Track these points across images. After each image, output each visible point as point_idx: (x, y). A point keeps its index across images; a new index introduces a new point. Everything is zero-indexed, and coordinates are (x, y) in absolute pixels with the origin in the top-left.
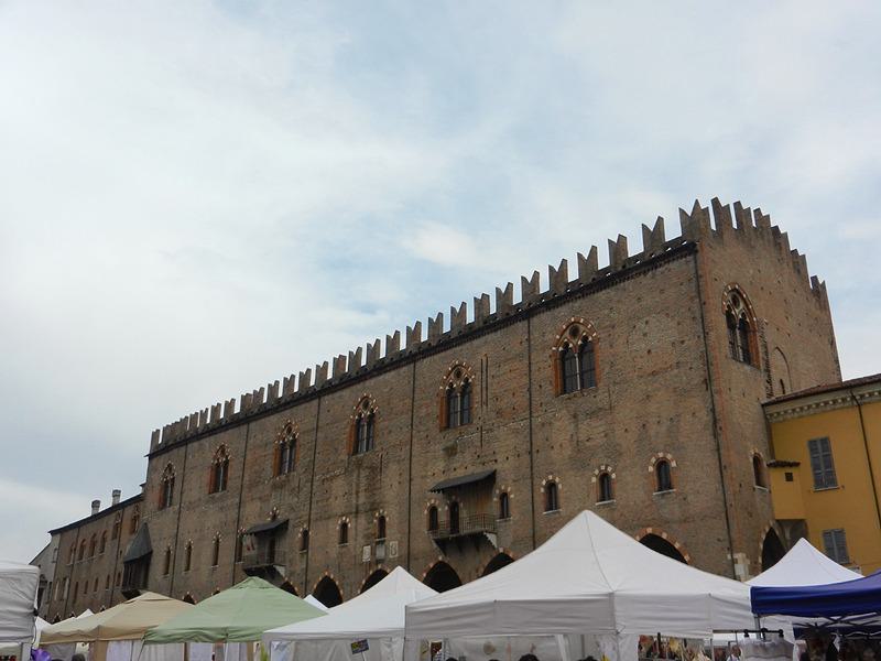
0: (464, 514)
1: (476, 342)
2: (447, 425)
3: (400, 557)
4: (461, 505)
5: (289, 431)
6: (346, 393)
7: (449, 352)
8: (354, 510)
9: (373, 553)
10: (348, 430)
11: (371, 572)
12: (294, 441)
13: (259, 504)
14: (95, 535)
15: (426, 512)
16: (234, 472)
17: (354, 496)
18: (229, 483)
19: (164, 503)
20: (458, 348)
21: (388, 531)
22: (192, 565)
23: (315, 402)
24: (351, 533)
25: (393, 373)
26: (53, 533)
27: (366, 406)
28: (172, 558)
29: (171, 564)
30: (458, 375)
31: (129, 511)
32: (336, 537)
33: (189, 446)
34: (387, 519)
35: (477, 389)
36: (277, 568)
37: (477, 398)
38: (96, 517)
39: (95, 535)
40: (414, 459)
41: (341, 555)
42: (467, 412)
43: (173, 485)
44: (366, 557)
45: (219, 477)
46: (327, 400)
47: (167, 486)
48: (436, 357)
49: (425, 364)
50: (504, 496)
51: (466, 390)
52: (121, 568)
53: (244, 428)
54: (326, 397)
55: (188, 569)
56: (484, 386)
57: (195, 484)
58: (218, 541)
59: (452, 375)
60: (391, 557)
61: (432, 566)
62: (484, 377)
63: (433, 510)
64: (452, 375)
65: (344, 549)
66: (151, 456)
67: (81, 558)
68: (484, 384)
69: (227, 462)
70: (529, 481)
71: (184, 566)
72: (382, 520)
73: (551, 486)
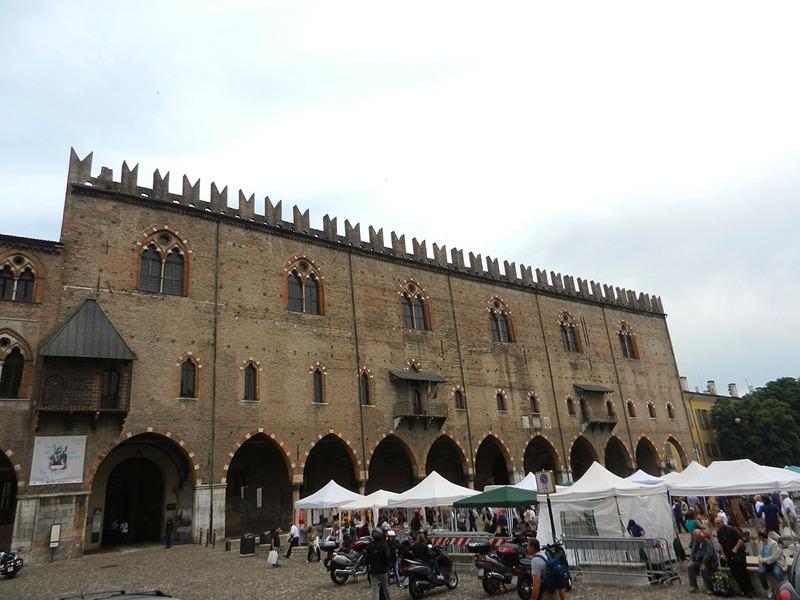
0: (590, 409)
1: (574, 304)
4: (587, 402)
7: (557, 300)
9: (531, 423)
11: (532, 437)
13: (387, 347)
17: (506, 374)
20: (564, 302)
21: (540, 408)
32: (495, 404)
35: (582, 334)
41: (500, 418)
44: (526, 424)
50: (609, 404)
58: (318, 374)
65: (504, 416)
66: (75, 190)
72: (533, 398)
73: (630, 405)
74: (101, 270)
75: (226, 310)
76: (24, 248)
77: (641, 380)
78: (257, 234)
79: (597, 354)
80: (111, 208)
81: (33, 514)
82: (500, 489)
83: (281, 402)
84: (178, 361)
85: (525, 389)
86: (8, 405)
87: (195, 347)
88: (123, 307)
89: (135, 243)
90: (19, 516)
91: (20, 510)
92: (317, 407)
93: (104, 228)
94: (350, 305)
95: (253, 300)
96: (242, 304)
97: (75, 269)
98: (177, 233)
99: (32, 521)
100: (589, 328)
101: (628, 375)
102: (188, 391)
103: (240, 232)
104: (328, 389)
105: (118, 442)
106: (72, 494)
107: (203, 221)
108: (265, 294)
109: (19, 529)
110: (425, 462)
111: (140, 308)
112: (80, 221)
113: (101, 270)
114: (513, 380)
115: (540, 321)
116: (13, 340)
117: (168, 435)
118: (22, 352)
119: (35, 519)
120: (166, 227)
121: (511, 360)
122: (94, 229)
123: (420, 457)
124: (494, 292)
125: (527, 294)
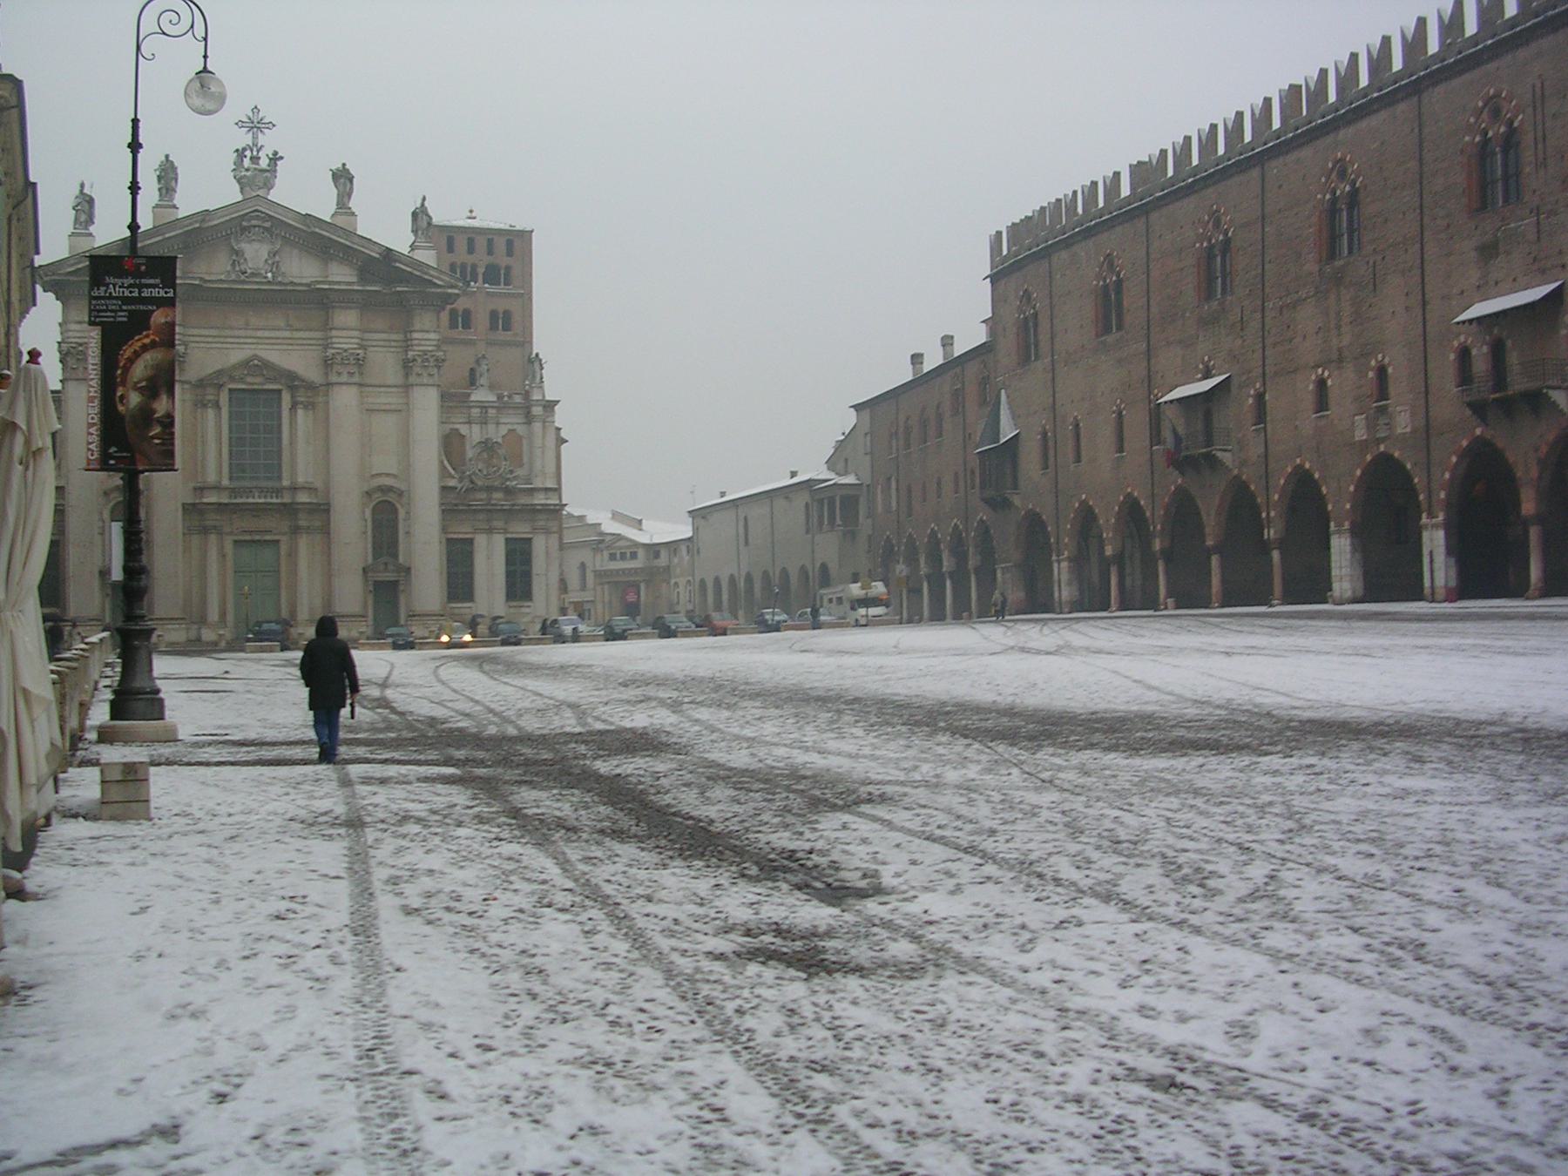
0: (1513, 359)
2: (1481, 202)
3: (1414, 431)
4: (1509, 343)
5: (1217, 224)
6: (1306, 153)
8: (1335, 357)
10: (1314, 219)
11: (1369, 458)
12: (1227, 241)
14: (924, 409)
15: (1452, 356)
16: (1132, 299)
18: (1128, 319)
19: (1027, 352)
20: (1491, 67)
21: (1392, 391)
22: (1083, 453)
23: (1255, 173)
24: (1334, 395)
25: (1383, 115)
26: (858, 407)
27: (1342, 174)
28: (1051, 444)
29: (1051, 453)
30: (1496, 113)
31: (973, 369)
32: (1309, 401)
33: (1055, 258)
34: (1390, 370)
35: (1528, 139)
36: (1219, 454)
37: (1528, 156)
38: (921, 381)
39: (924, 409)
40: (1428, 268)
42: (1512, 179)
43: (1036, 325)
44: (1360, 434)
45: (1109, 309)
46: (1275, 167)
47: (1028, 330)
48: (1456, 82)
49: (1436, 97)
51: (1510, 142)
52: (975, 463)
53: (1140, 224)
54: (1274, 163)
55: (1078, 460)
56: (1540, 134)
57: (1074, 322)
58: (1120, 414)
59: (1485, 115)
60: (1399, 431)
61: (1465, 443)
62: (1539, 117)
63: (1464, 354)
64: (1485, 115)
65: (1323, 422)
66: (995, 278)
67: (908, 446)
68: (1540, 127)
69: (1119, 282)
71: (1071, 457)
72: (1382, 371)
82: (1167, 573)
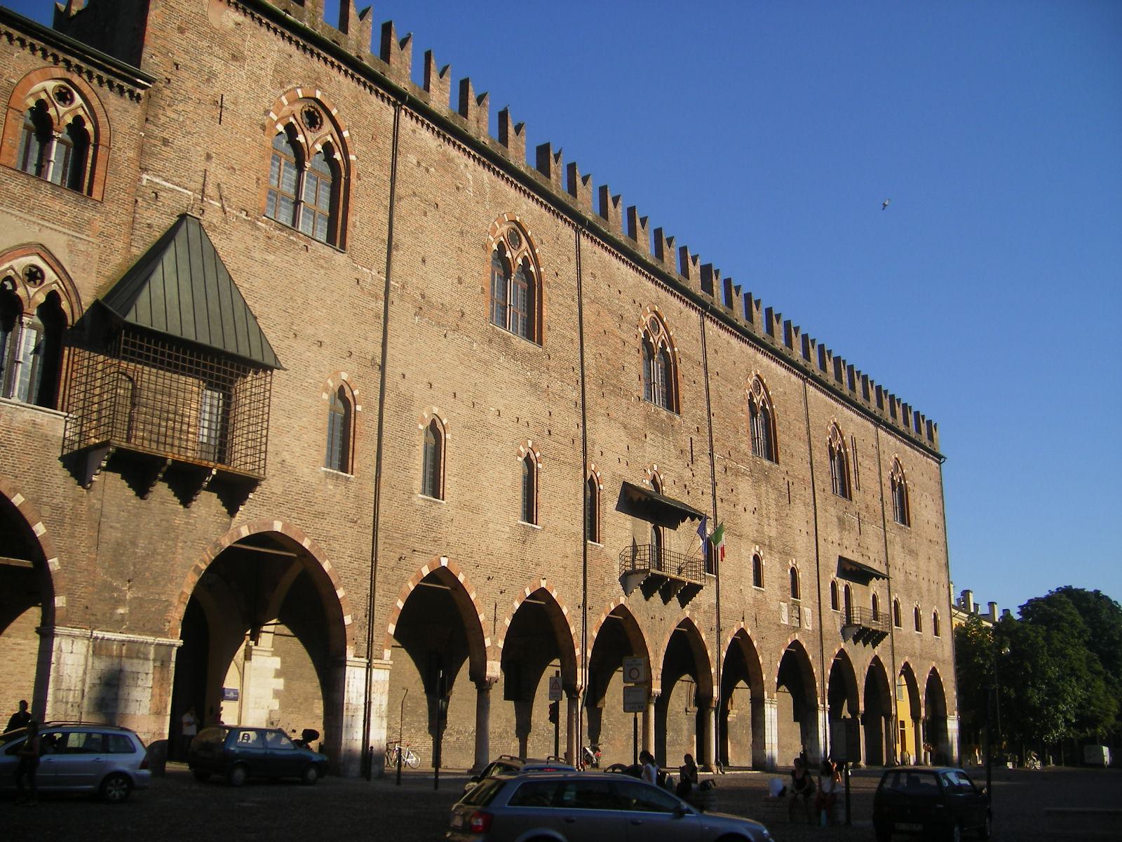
13: (622, 433)
17: (765, 520)
44: (785, 620)
63: (834, 585)
65: (760, 596)
70: (887, 591)
74: (209, 157)
75: (402, 297)
76: (79, 70)
77: (910, 566)
78: (453, 152)
79: (867, 507)
80: (231, 25)
81: (81, 672)
83: (475, 510)
84: (326, 389)
85: (786, 553)
86: (38, 421)
87: (352, 365)
88: (241, 247)
89: (267, 112)
90: (58, 672)
91: (59, 659)
92: (527, 532)
93: (218, 66)
94: (576, 336)
95: (440, 286)
96: (427, 293)
97: (165, 142)
98: (334, 112)
99: (79, 686)
100: (860, 459)
101: (897, 553)
102: (342, 457)
103: (427, 138)
104: (542, 497)
105: (226, 542)
106: (150, 639)
107: (373, 97)
108: (460, 281)
109: (56, 701)
110: (661, 667)
111: (271, 257)
112: (176, 37)
113: (209, 157)
114: (773, 534)
115: (809, 433)
116: (50, 275)
117: (306, 544)
118: (65, 305)
119: (84, 681)
120: (318, 95)
121: (773, 495)
122: (199, 61)
123: (657, 655)
124: (756, 362)
125: (794, 378)
